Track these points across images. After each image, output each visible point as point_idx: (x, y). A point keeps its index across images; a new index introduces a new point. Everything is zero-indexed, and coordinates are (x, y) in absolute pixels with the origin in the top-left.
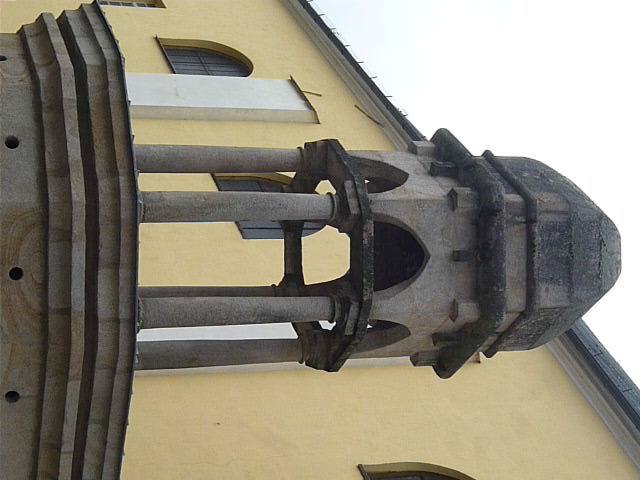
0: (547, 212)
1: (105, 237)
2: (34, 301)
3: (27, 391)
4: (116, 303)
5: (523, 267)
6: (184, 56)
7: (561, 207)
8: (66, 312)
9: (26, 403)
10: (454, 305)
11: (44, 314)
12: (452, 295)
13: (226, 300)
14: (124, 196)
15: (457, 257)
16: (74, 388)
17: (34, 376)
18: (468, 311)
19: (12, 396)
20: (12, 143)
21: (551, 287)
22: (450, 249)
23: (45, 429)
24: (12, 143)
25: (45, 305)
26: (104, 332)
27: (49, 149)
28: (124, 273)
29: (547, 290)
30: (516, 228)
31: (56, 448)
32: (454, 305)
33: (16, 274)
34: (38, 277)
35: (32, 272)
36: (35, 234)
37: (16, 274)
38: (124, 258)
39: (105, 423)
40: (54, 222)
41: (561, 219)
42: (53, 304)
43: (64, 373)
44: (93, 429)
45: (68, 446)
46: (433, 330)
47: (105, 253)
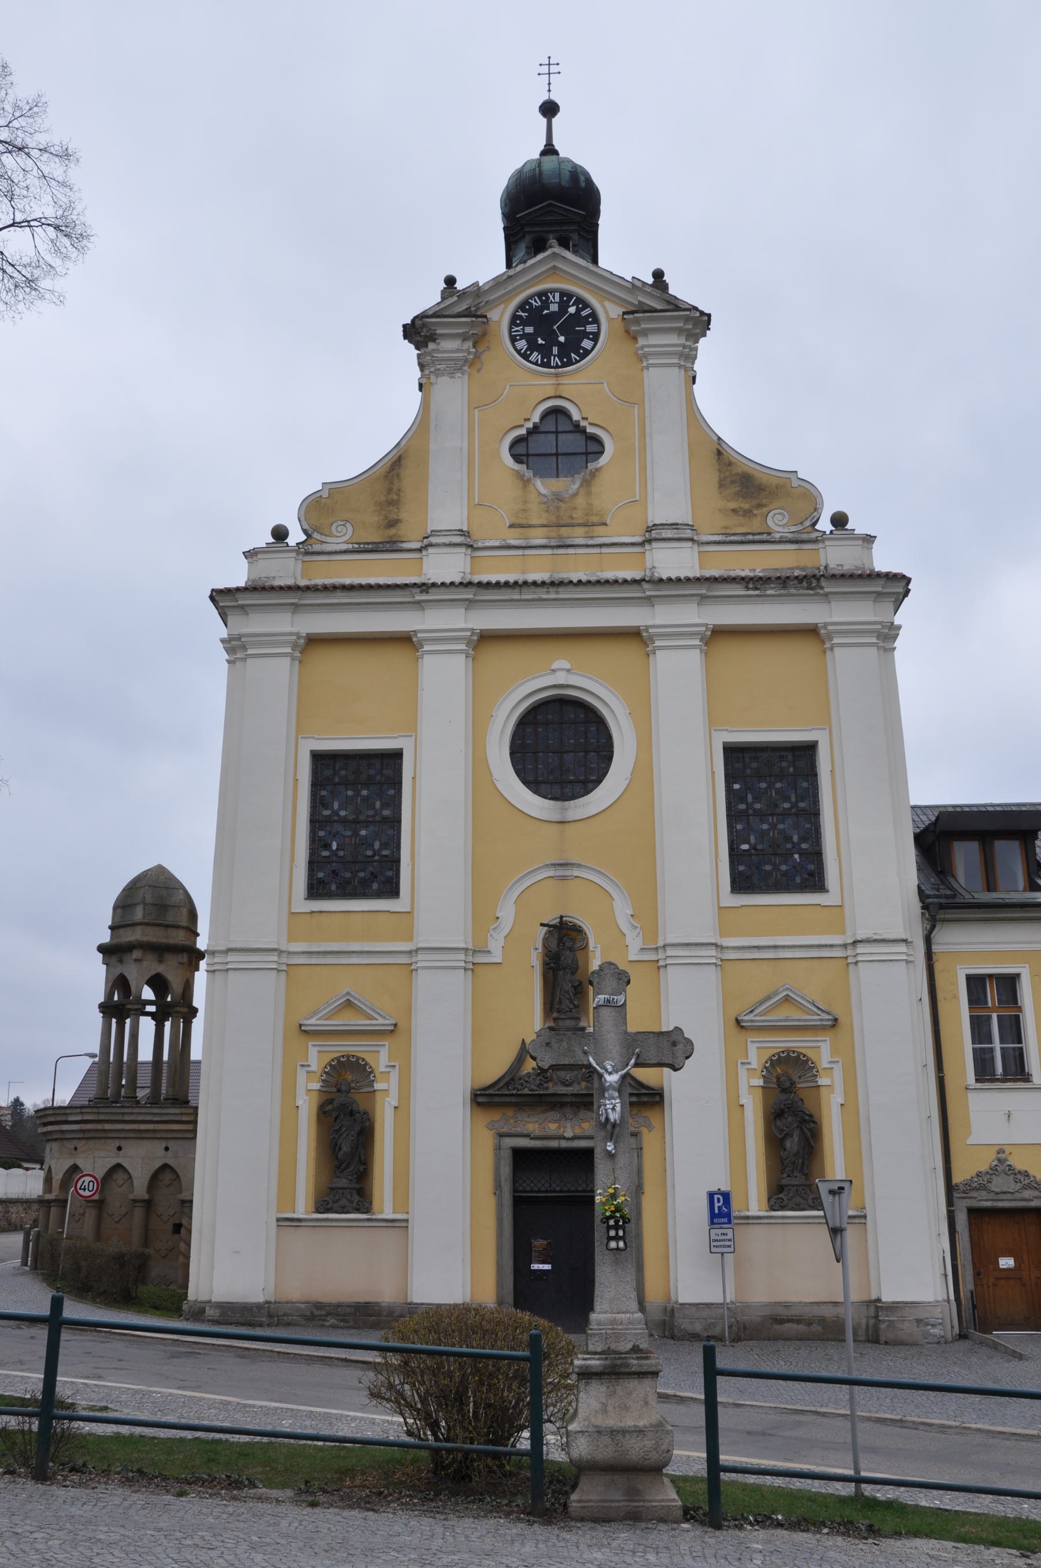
1: (59, 1118)
2: (84, 1142)
3: (117, 1143)
9: (123, 1143)
10: (136, 960)
11: (88, 1138)
15: (121, 961)
16: (107, 1126)
17: (111, 1141)
18: (136, 954)
19: (119, 1148)
23: (132, 1135)
26: (86, 1117)
28: (68, 1111)
31: (140, 1131)
32: (136, 960)
35: (75, 1143)
37: (76, 1149)
39: (123, 1114)
43: (104, 1131)
44: (127, 1118)
45: (135, 1127)
47: (63, 1118)
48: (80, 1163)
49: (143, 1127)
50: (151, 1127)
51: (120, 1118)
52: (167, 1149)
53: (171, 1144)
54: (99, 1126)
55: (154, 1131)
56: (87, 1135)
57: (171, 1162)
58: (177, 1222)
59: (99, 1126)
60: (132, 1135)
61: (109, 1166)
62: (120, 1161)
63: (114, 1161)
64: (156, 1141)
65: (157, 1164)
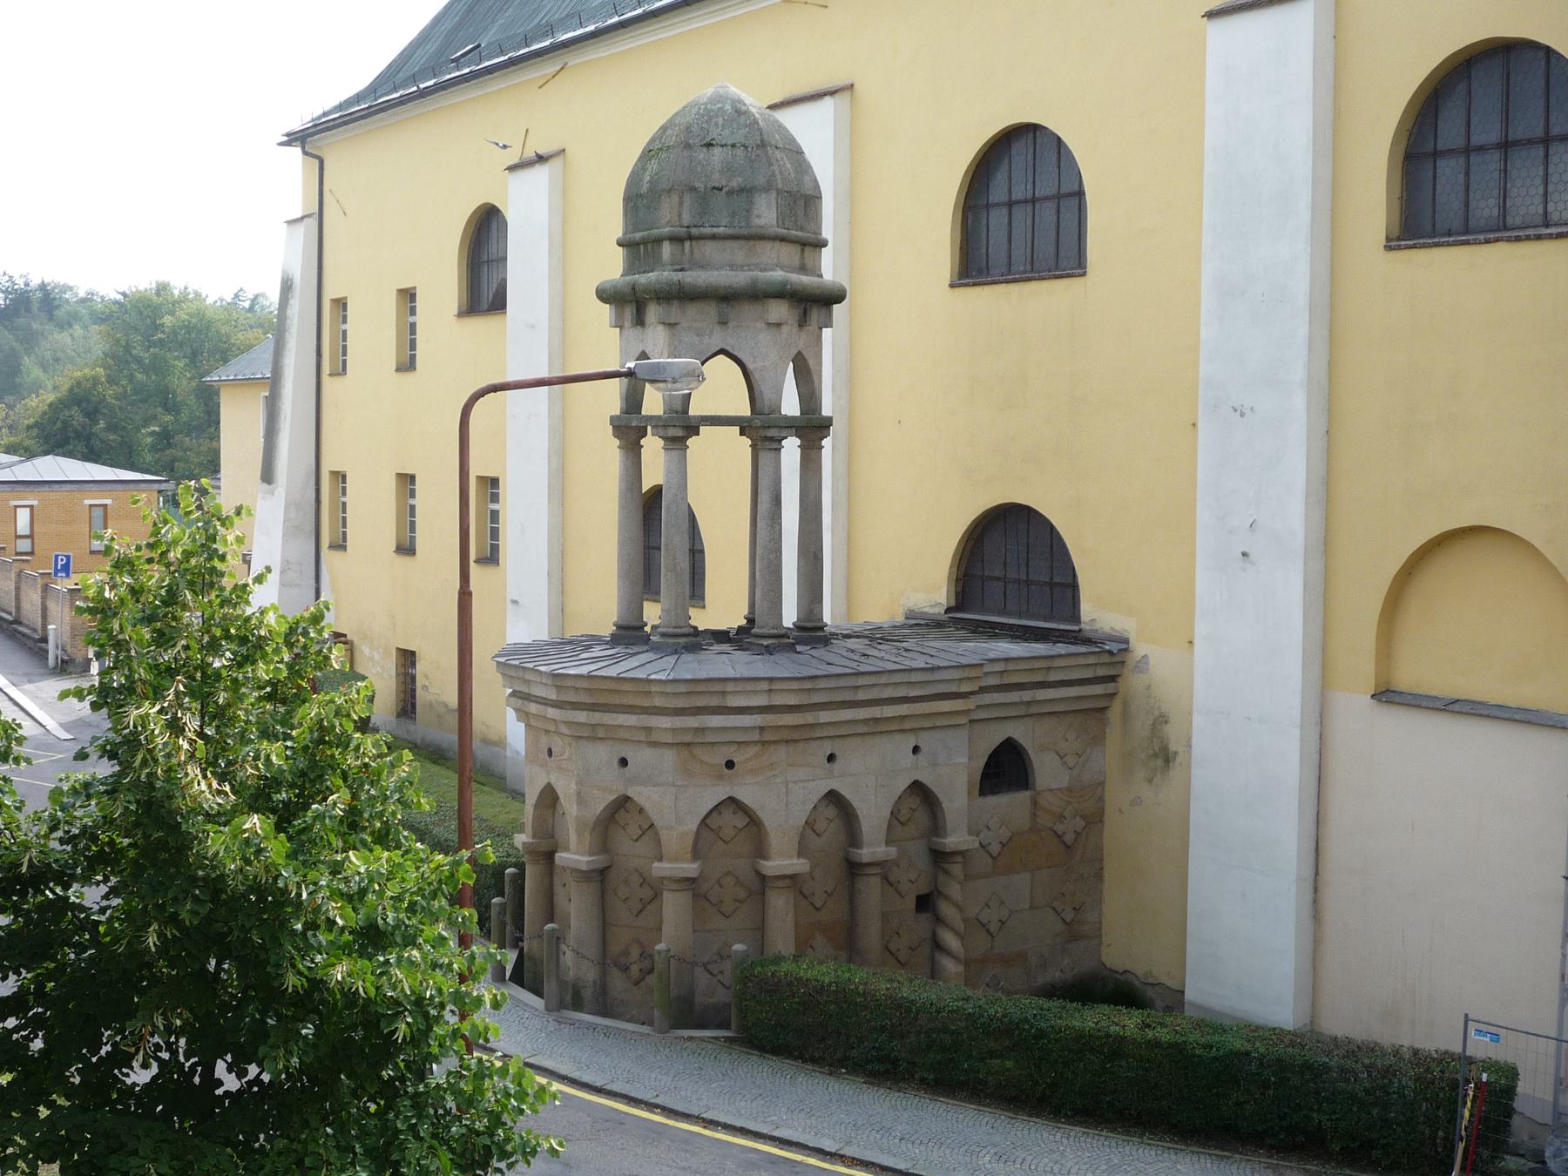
0: (680, 215)
2: (752, 751)
4: (755, 692)
5: (735, 244)
6: (483, 292)
7: (675, 198)
8: (762, 729)
12: (760, 325)
13: (759, 551)
14: (669, 689)
16: (825, 716)
17: (814, 744)
19: (831, 758)
20: (624, 762)
21: (755, 212)
22: (718, 328)
23: (861, 729)
24: (624, 762)
25: (756, 743)
26: (778, 700)
27: (627, 736)
29: (759, 216)
30: (696, 252)
31: (877, 720)
33: (730, 764)
34: (734, 748)
36: (697, 751)
37: (730, 764)
38: (717, 687)
40: (688, 738)
41: (687, 199)
42: (756, 738)
43: (812, 726)
44: (862, 696)
46: (795, 329)
47: (714, 702)
48: (746, 795)
49: (889, 711)
50: (902, 710)
51: (848, 696)
52: (916, 750)
53: (924, 740)
54: (809, 718)
55: (903, 718)
56: (768, 737)
57: (926, 778)
58: (924, 891)
59: (809, 718)
60: (861, 729)
61: (815, 798)
62: (834, 784)
63: (823, 787)
64: (897, 737)
65: (903, 783)
